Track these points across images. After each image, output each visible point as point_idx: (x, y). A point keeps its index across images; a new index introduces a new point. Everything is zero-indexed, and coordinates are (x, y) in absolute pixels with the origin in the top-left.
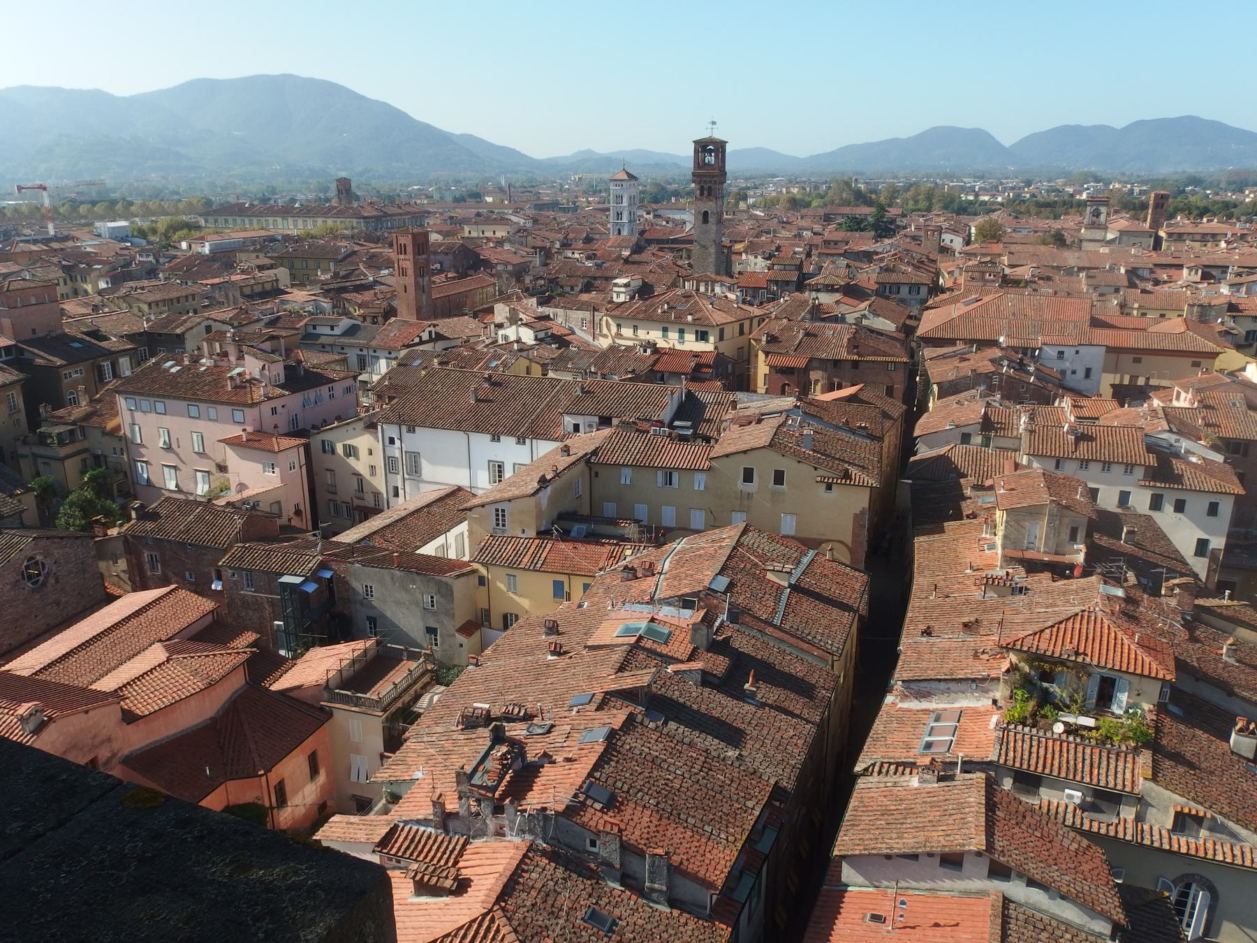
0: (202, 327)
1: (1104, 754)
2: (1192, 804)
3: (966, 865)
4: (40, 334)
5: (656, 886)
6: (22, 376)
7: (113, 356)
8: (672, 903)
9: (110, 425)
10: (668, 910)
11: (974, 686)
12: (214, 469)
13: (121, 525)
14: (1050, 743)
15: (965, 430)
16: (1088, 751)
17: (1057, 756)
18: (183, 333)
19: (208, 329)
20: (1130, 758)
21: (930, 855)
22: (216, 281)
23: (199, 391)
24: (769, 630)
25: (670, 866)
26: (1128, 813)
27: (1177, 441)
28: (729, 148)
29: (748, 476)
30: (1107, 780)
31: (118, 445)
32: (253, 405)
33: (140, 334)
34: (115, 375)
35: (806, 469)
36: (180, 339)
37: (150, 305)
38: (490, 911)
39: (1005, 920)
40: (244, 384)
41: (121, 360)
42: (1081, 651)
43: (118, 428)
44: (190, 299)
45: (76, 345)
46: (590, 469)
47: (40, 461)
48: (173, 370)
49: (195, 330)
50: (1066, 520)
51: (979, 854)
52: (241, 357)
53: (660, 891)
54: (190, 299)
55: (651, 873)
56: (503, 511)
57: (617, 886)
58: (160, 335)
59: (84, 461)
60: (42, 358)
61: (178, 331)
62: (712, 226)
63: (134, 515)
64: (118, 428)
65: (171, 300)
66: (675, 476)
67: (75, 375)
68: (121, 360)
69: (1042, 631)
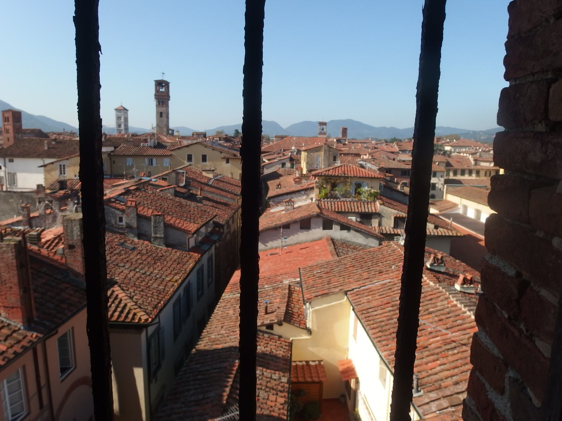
1: (362, 204)
2: (400, 213)
3: (312, 225)
5: (158, 235)
8: (167, 245)
10: (166, 248)
11: (303, 192)
14: (339, 203)
15: (283, 161)
16: (355, 203)
17: (343, 206)
20: (372, 204)
21: (295, 222)
24: (206, 188)
25: (165, 223)
26: (375, 222)
27: (366, 164)
28: (170, 85)
29: (190, 158)
30: (364, 209)
35: (216, 153)
38: (59, 236)
39: (333, 242)
42: (346, 173)
46: (111, 159)
50: (331, 153)
51: (318, 216)
53: (161, 238)
55: (155, 227)
56: (64, 166)
57: (136, 240)
62: (164, 118)
66: (154, 161)
69: (329, 170)
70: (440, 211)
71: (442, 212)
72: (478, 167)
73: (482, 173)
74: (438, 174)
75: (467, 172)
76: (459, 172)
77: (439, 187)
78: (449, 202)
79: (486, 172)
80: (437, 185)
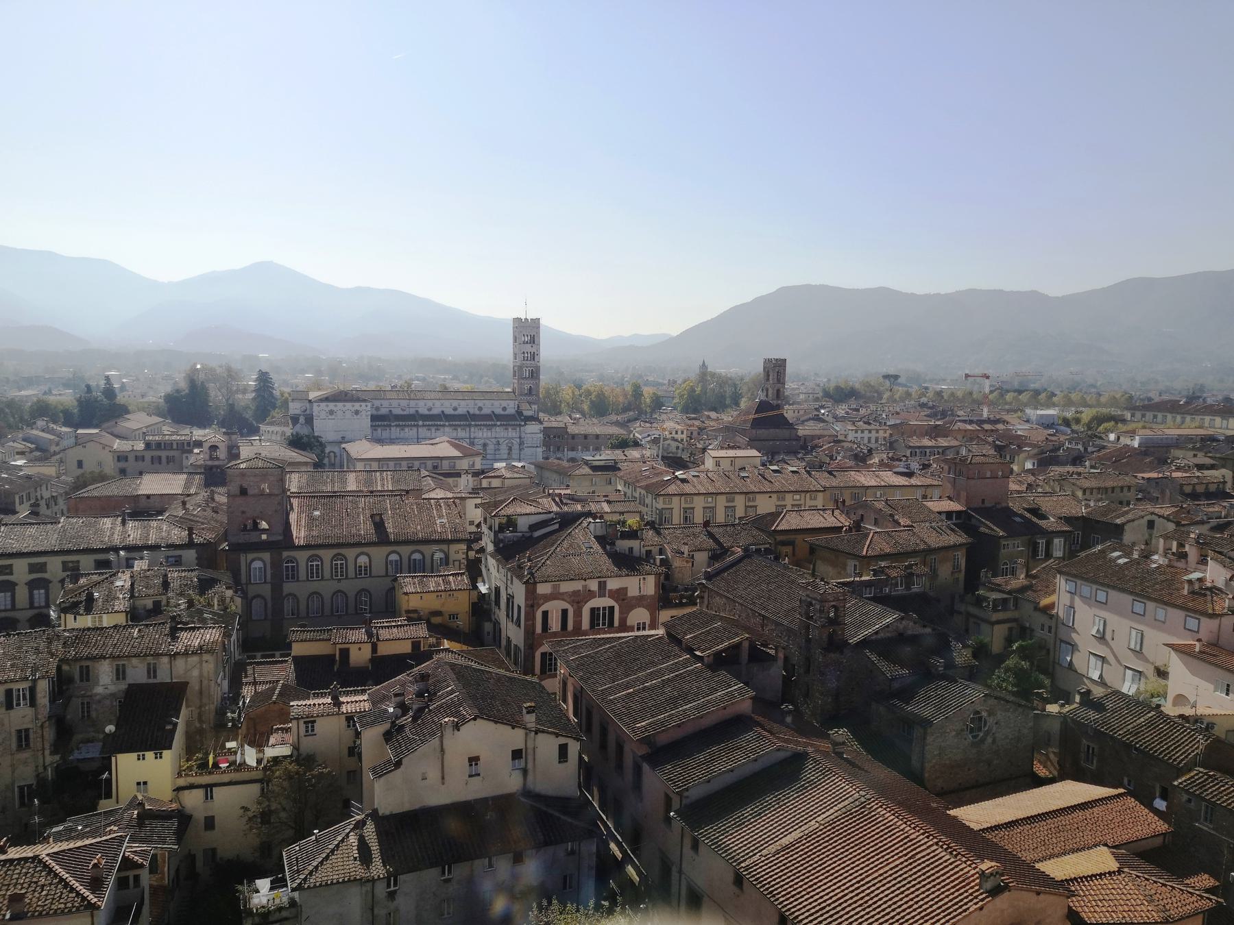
0: (1144, 522)
4: (988, 504)
6: (970, 540)
7: (1050, 535)
9: (1045, 602)
12: (1149, 671)
13: (1062, 706)
18: (1123, 524)
19: (1151, 524)
22: (1154, 475)
23: (1148, 588)
31: (1047, 622)
32: (1213, 616)
33: (1077, 518)
34: (1048, 555)
36: (1119, 530)
37: (1084, 491)
40: (1203, 592)
41: (1056, 541)
43: (1052, 606)
44: (1125, 490)
45: (1018, 519)
47: (972, 620)
48: (1121, 561)
49: (1136, 523)
52: (1203, 561)
54: (1125, 490)
58: (1098, 522)
59: (1010, 629)
60: (989, 528)
61: (1118, 521)
63: (1078, 698)
64: (1052, 606)
65: (1106, 489)
67: (1014, 547)
68: (1056, 541)
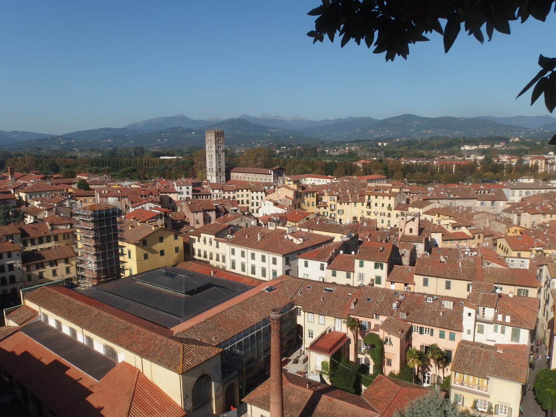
70: (20, 325)
71: (23, 325)
72: (56, 232)
73: (60, 237)
74: (13, 254)
75: (45, 239)
76: (37, 241)
77: (18, 266)
78: (28, 308)
79: (64, 236)
80: (15, 265)
